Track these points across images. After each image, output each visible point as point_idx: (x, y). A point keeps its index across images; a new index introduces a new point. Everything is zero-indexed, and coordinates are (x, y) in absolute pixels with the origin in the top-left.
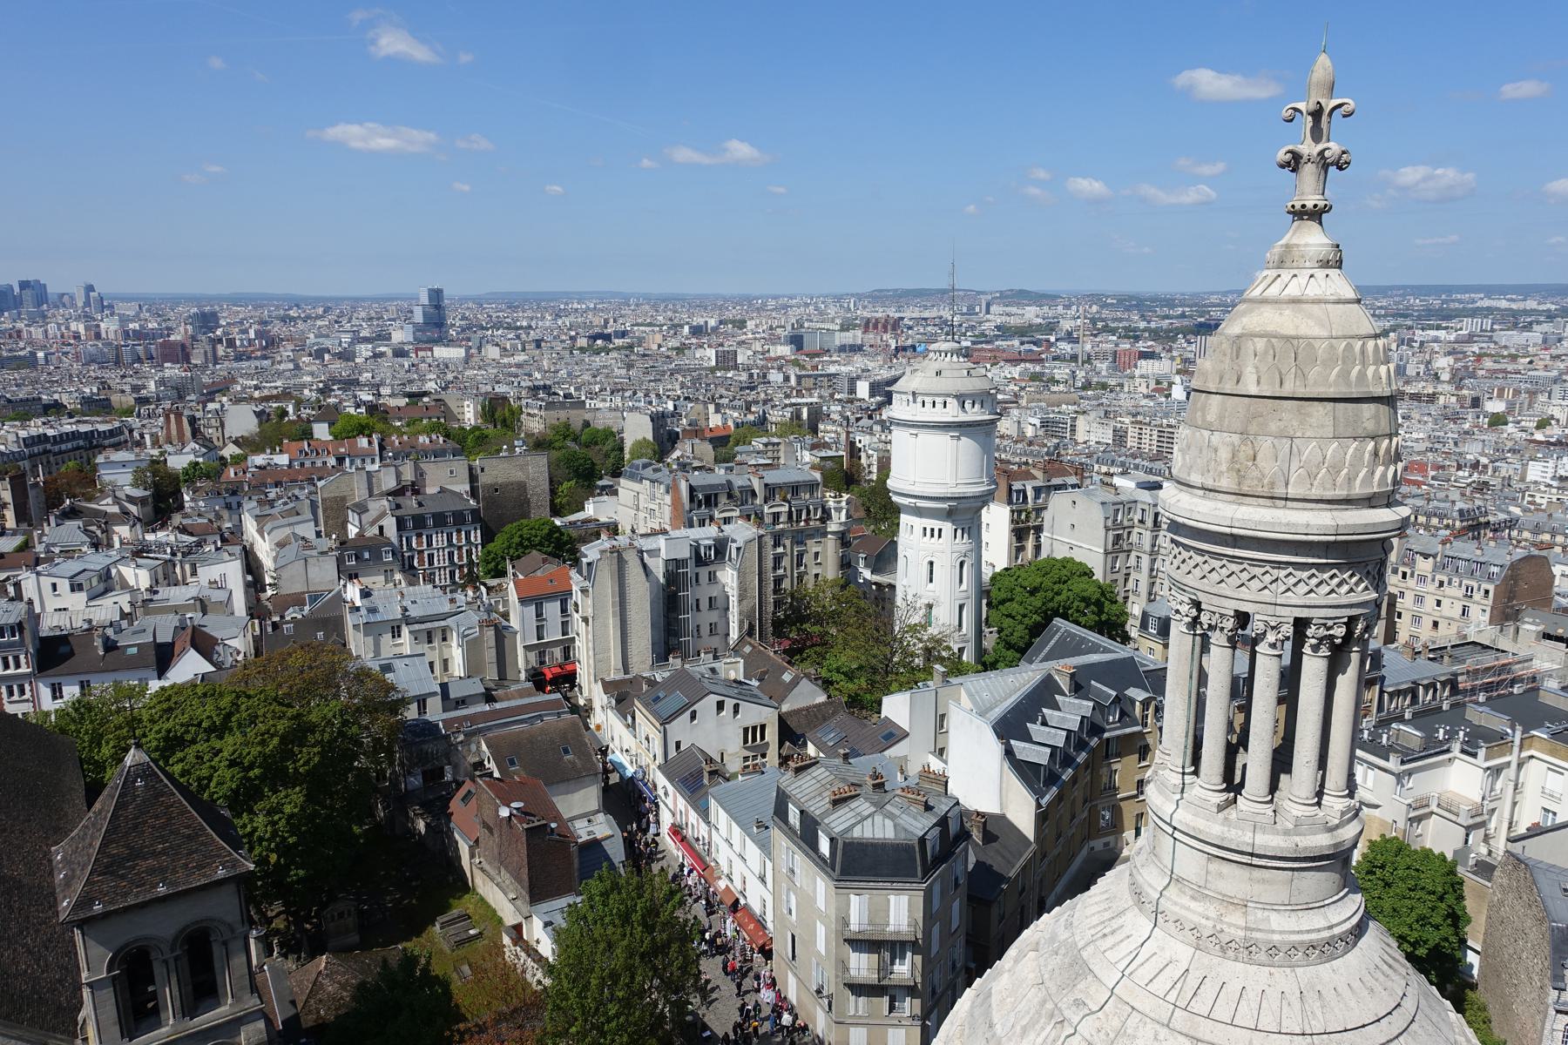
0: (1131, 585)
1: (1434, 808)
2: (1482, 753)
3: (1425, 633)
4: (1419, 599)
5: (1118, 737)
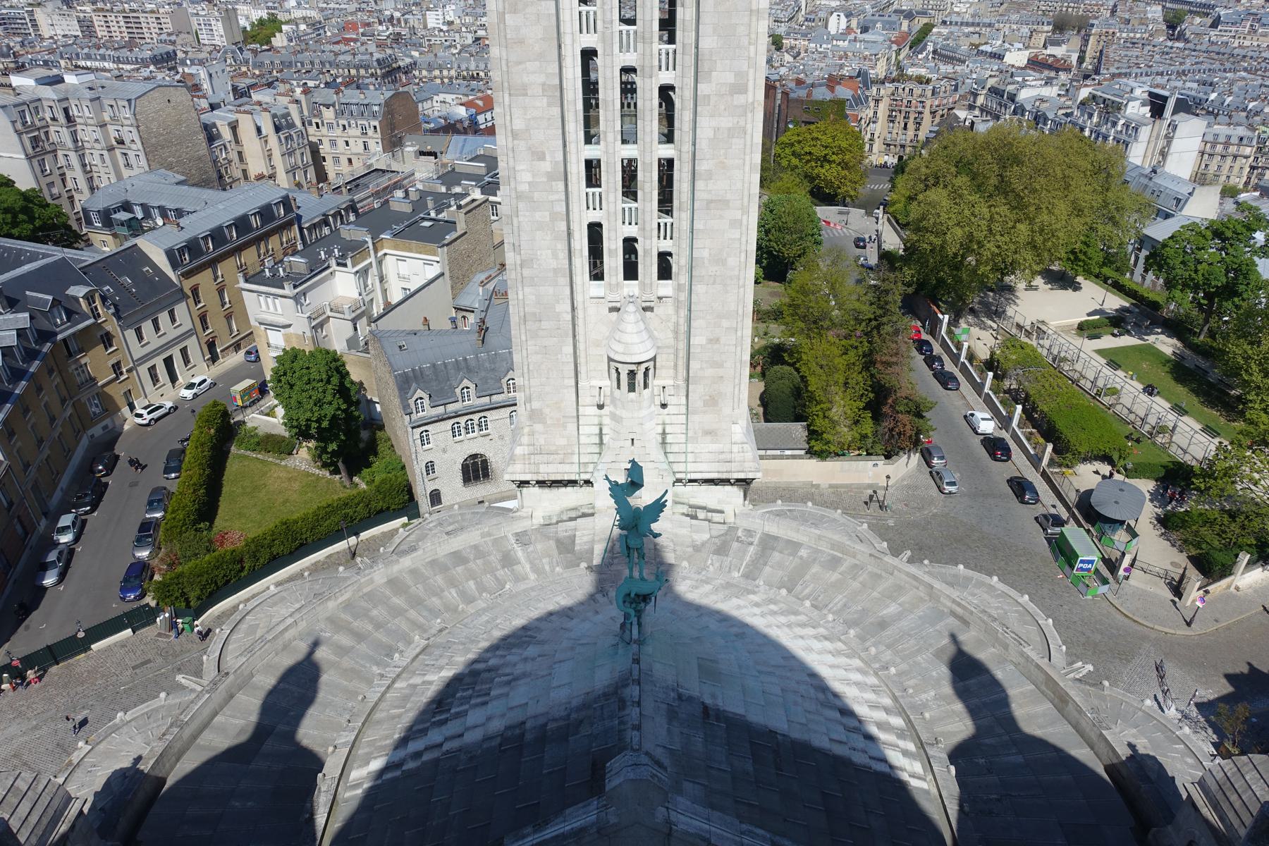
0: (70, 185)
1: (329, 313)
2: (349, 262)
3: (344, 167)
4: (333, 143)
5: (74, 334)
